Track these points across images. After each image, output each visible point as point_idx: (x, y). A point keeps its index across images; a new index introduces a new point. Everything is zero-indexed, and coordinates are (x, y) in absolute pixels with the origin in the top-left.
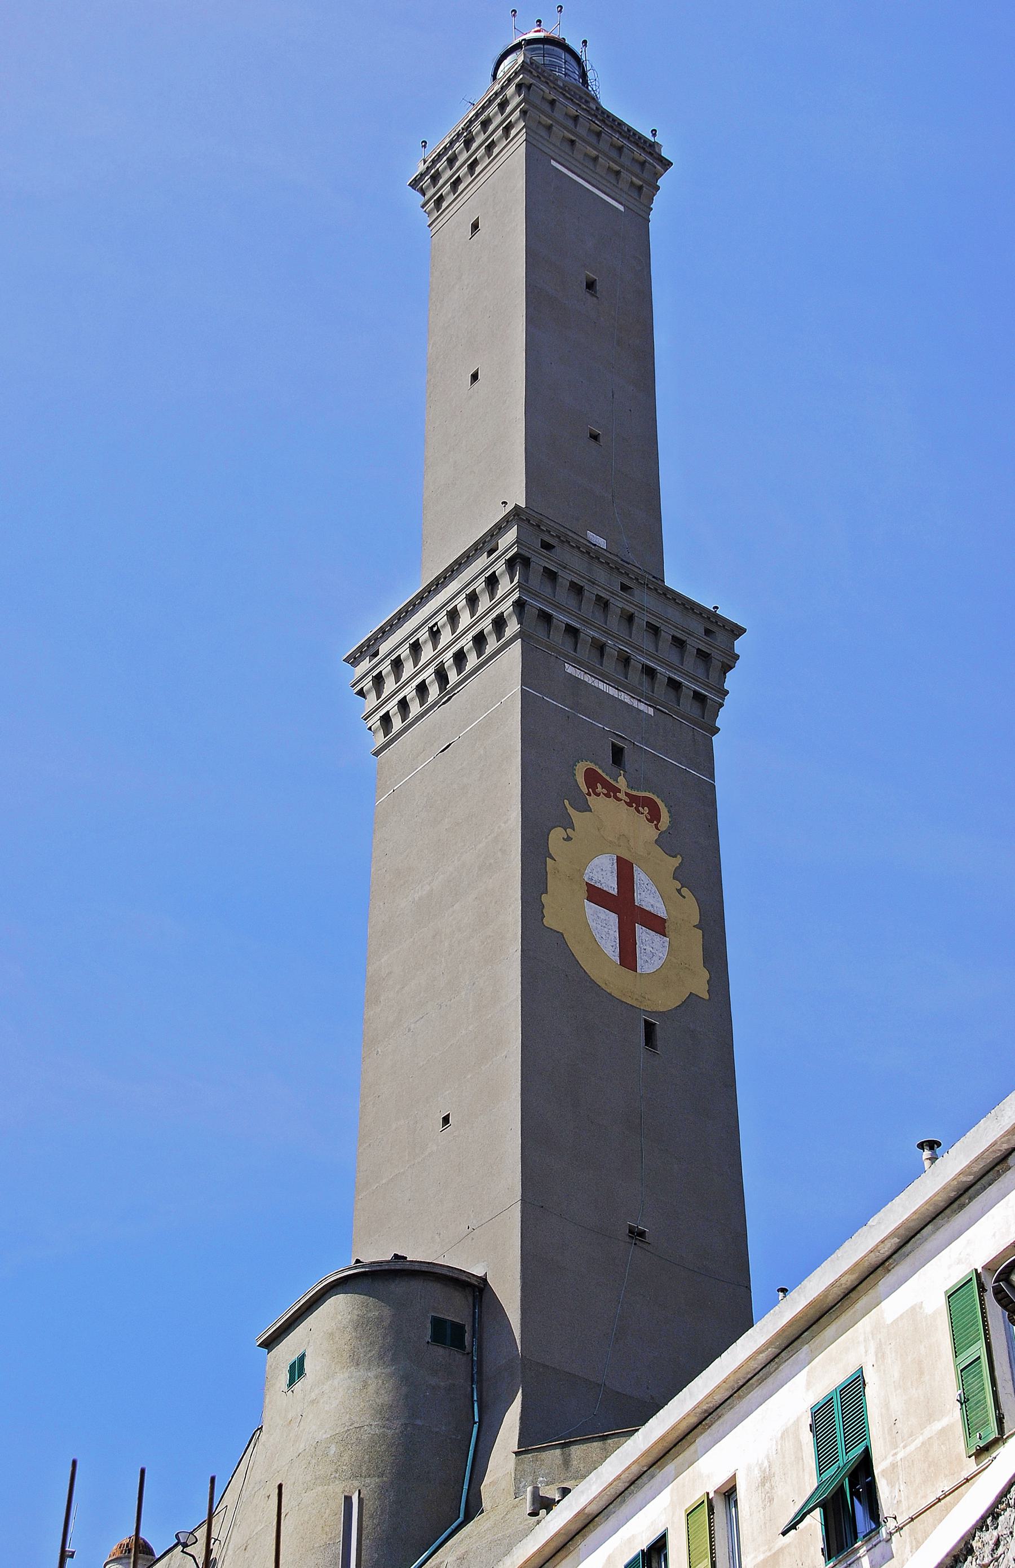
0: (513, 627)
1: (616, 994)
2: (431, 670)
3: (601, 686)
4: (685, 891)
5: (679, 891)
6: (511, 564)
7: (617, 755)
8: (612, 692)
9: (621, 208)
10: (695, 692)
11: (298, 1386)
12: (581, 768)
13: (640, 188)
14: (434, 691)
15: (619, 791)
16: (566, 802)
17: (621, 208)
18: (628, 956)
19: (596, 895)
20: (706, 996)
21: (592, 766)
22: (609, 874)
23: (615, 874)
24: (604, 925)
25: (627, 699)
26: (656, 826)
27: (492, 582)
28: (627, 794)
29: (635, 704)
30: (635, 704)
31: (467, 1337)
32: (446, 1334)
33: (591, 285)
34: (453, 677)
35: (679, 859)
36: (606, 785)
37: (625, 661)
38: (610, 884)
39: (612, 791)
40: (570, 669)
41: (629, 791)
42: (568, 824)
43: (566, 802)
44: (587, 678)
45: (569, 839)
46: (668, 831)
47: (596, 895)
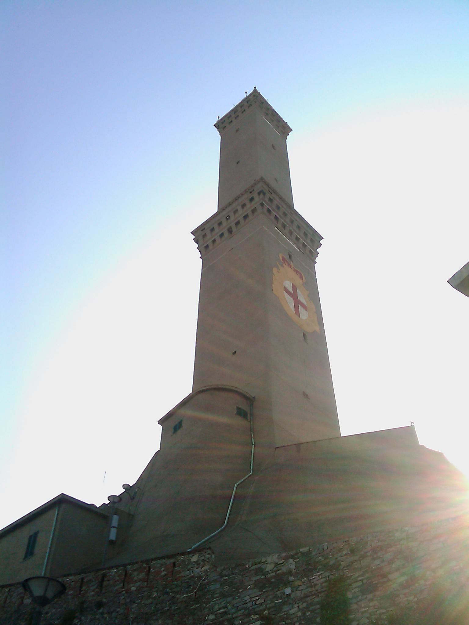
0: (259, 210)
2: (226, 229)
6: (259, 193)
11: (179, 432)
12: (281, 255)
14: (226, 234)
24: (290, 302)
27: (252, 199)
31: (249, 416)
32: (241, 413)
34: (234, 229)
36: (287, 262)
37: (291, 233)
38: (291, 290)
39: (289, 265)
42: (278, 268)
45: (278, 272)
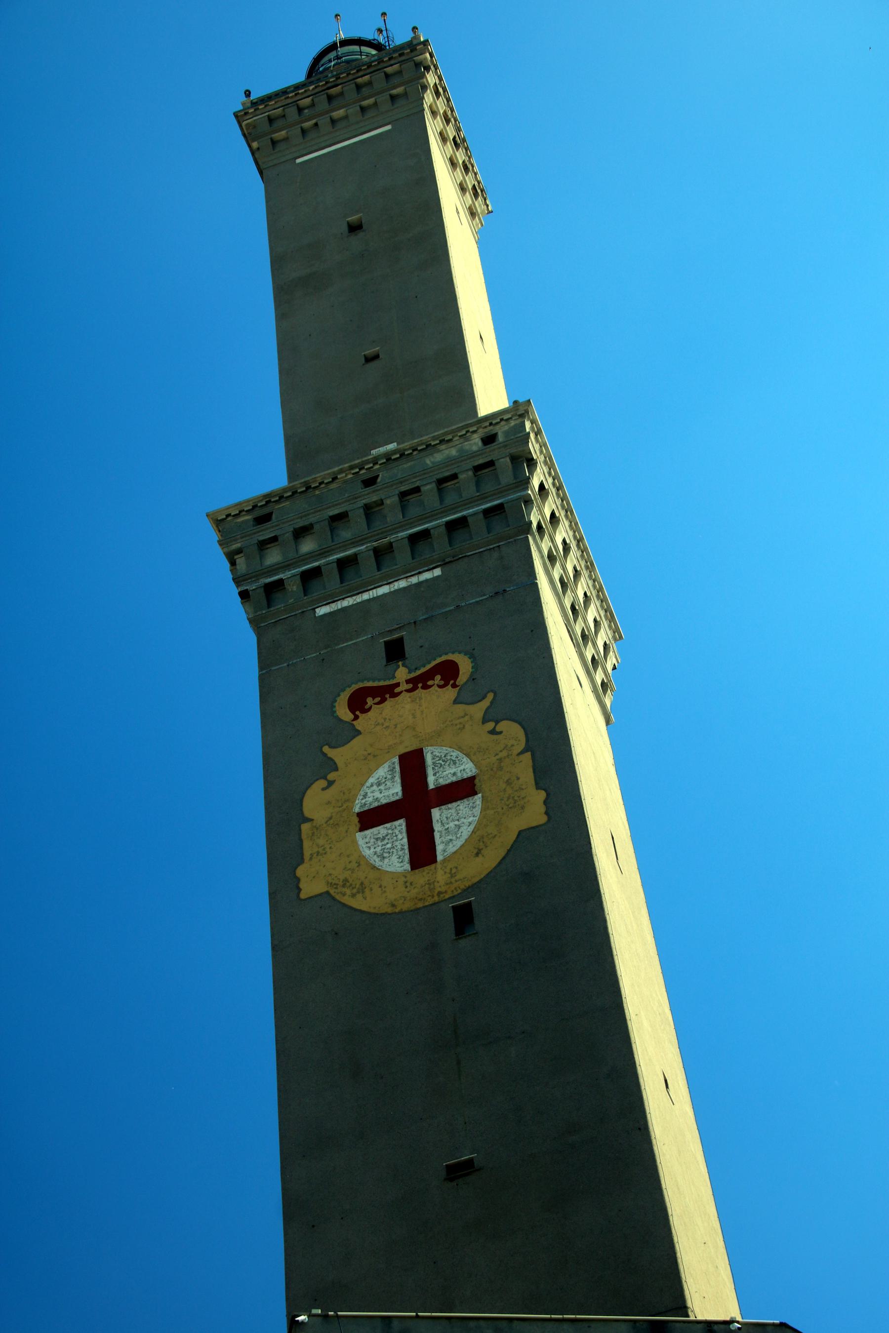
1: (407, 906)
3: (366, 596)
4: (503, 726)
5: (493, 732)
7: (395, 651)
8: (384, 590)
9: (389, 127)
10: (487, 512)
13: (405, 95)
15: (398, 685)
16: (326, 749)
17: (389, 127)
18: (422, 851)
19: (372, 818)
20: (543, 819)
21: (361, 685)
22: (388, 783)
23: (398, 779)
25: (402, 584)
26: (454, 686)
28: (408, 682)
29: (414, 580)
30: (414, 580)
33: (354, 228)
35: (490, 696)
38: (394, 791)
39: (387, 692)
40: (321, 611)
41: (413, 675)
43: (326, 749)
44: (346, 603)
45: (331, 783)
46: (472, 679)
47: (372, 818)
